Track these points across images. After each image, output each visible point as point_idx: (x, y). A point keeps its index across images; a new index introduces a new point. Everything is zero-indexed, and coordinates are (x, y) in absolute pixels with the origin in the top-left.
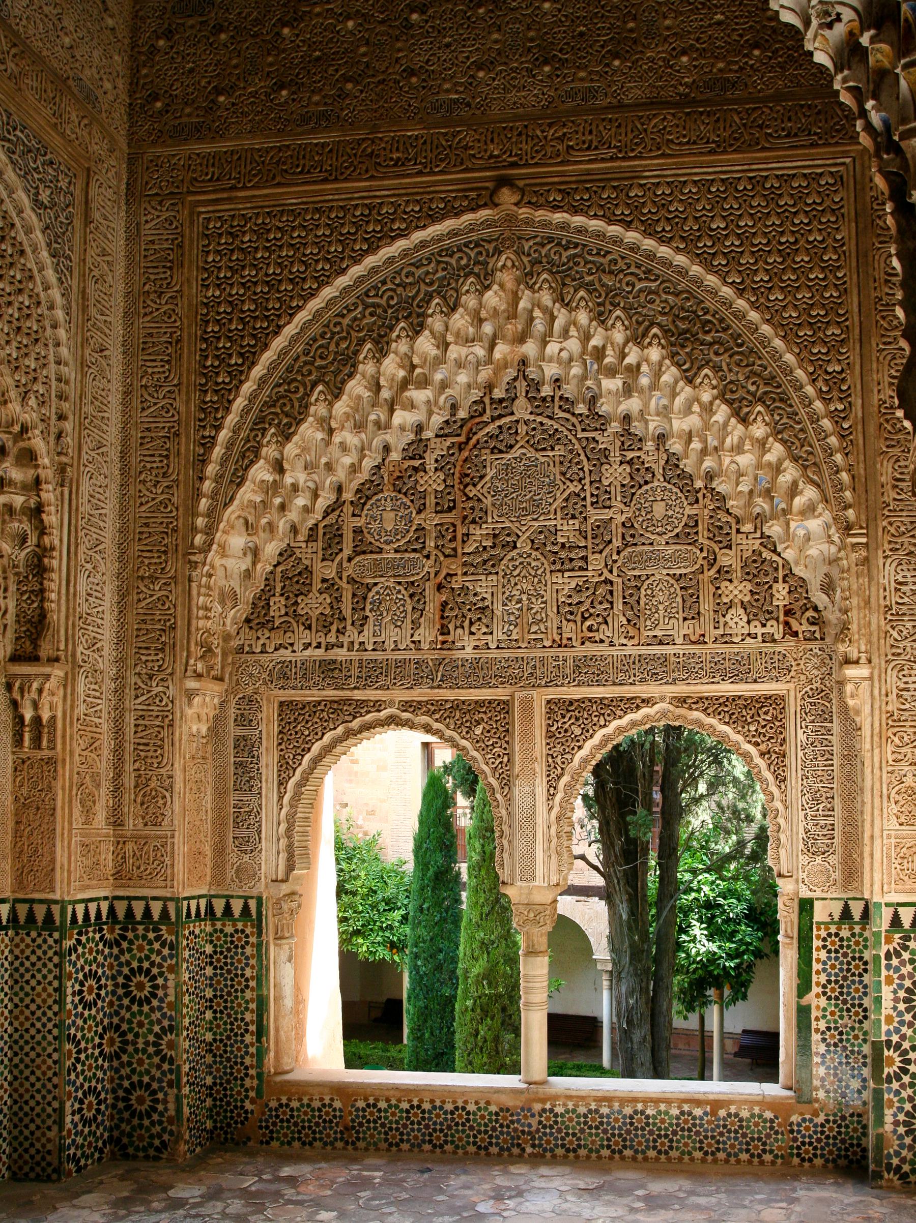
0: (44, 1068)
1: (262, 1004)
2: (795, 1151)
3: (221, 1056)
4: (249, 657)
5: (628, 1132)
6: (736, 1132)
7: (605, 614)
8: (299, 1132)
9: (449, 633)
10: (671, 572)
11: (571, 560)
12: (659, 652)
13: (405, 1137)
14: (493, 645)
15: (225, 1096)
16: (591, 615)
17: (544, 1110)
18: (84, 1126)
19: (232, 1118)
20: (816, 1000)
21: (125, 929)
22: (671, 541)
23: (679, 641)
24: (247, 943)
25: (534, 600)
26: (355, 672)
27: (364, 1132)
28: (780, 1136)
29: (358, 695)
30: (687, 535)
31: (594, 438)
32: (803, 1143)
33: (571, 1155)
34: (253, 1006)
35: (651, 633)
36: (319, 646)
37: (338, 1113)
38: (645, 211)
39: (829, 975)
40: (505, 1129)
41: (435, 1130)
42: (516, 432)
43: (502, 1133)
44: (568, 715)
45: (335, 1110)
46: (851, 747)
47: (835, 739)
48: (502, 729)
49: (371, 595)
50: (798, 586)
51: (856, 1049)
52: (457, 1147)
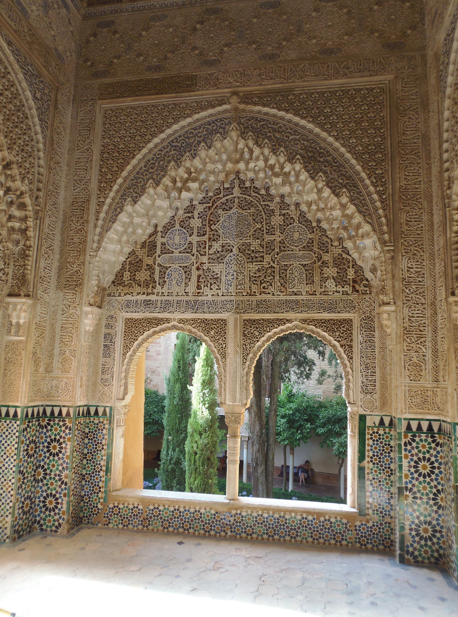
0: (7, 486)
2: (358, 540)
3: (89, 482)
5: (277, 526)
6: (329, 529)
7: (271, 281)
10: (301, 263)
11: (256, 257)
14: (220, 294)
15: (89, 501)
17: (237, 514)
18: (23, 515)
19: (92, 512)
21: (50, 420)
25: (239, 275)
26: (159, 305)
28: (350, 532)
29: (160, 316)
30: (308, 247)
32: (362, 536)
33: (249, 537)
34: (105, 458)
35: (291, 290)
37: (140, 511)
38: (295, 105)
39: (374, 452)
40: (218, 523)
41: (185, 522)
42: (234, 202)
43: (217, 524)
45: (139, 510)
46: (384, 344)
47: (376, 340)
48: (223, 332)
49: (167, 272)
50: (359, 270)
52: (195, 530)
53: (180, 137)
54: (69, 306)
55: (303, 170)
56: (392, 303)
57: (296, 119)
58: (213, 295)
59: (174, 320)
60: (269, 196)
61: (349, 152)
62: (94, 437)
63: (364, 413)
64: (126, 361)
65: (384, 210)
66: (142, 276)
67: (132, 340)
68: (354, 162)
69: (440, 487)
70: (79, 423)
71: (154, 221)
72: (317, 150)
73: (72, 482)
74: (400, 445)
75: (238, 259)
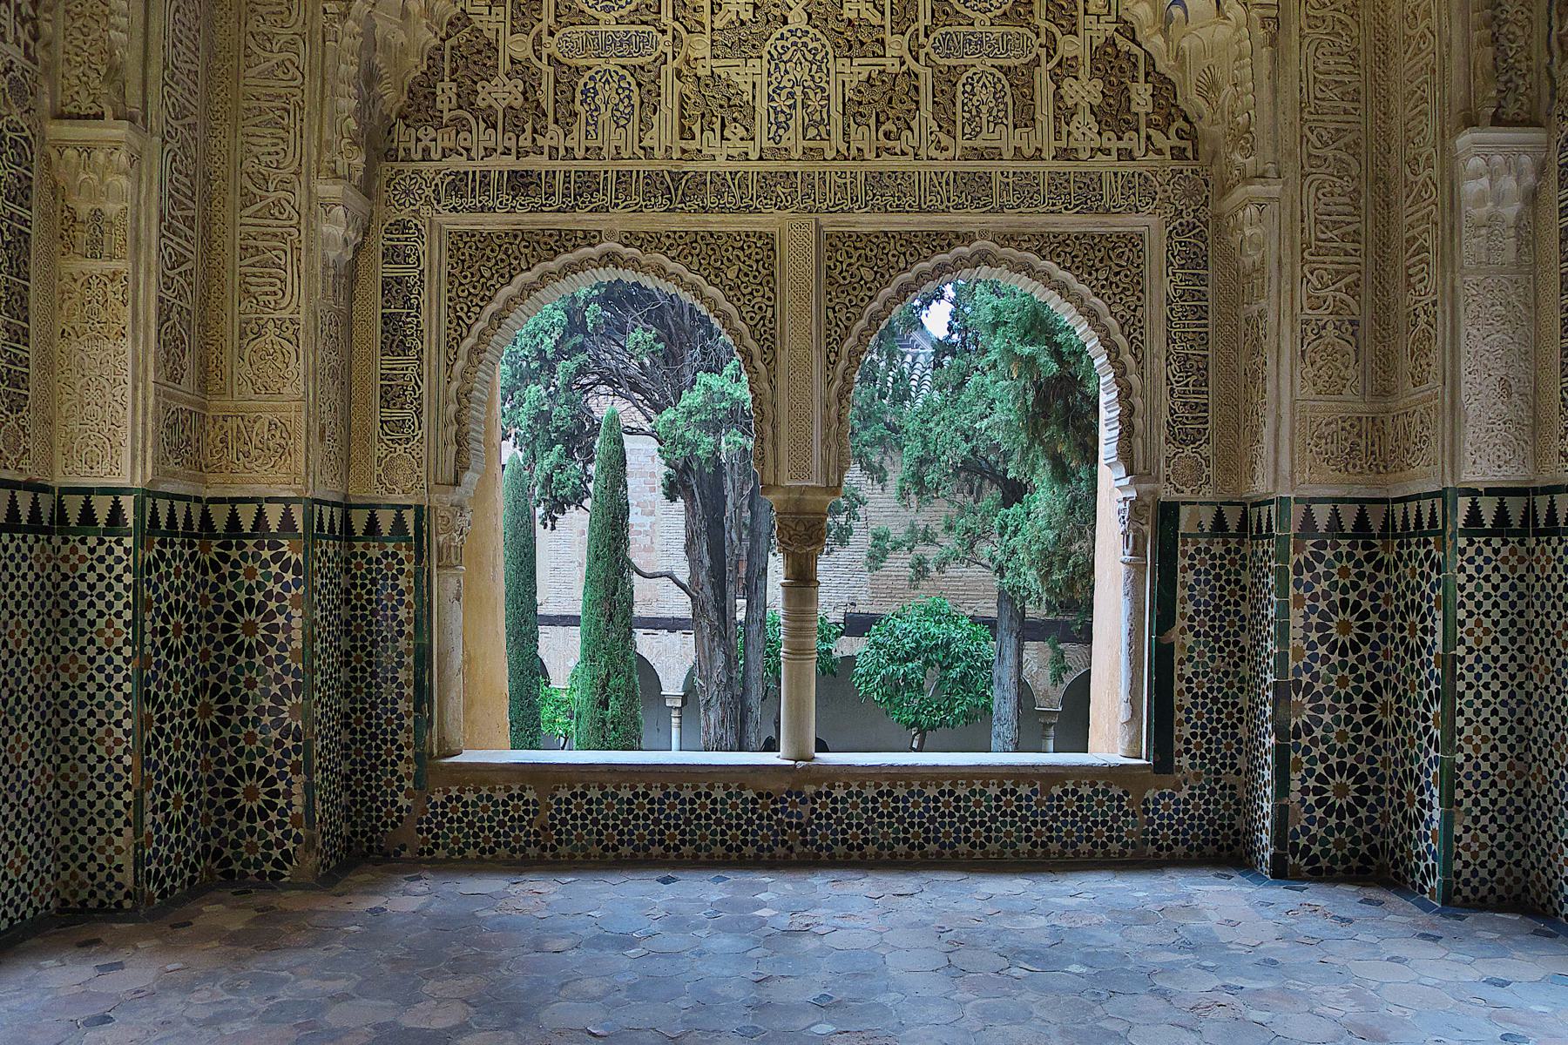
1: (423, 657)
2: (1150, 837)
4: (409, 168)
6: (1074, 814)
8: (476, 835)
9: (693, 138)
10: (997, 62)
11: (862, 44)
15: (369, 787)
16: (888, 119)
17: (819, 794)
19: (379, 818)
20: (1181, 638)
22: (996, 21)
24: (401, 571)
25: (812, 95)
27: (569, 833)
28: (1130, 818)
29: (564, 221)
32: (1161, 826)
34: (409, 660)
35: (968, 144)
36: (506, 152)
37: (531, 808)
40: (765, 822)
41: (668, 826)
43: (761, 827)
45: (526, 803)
48: (764, 272)
50: (1164, 88)
51: (1230, 700)
52: (699, 848)
56: (1272, 174)
58: (730, 158)
62: (369, 601)
63: (1175, 496)
64: (460, 364)
66: (501, 93)
69: (1380, 678)
73: (317, 728)
74: (1282, 574)
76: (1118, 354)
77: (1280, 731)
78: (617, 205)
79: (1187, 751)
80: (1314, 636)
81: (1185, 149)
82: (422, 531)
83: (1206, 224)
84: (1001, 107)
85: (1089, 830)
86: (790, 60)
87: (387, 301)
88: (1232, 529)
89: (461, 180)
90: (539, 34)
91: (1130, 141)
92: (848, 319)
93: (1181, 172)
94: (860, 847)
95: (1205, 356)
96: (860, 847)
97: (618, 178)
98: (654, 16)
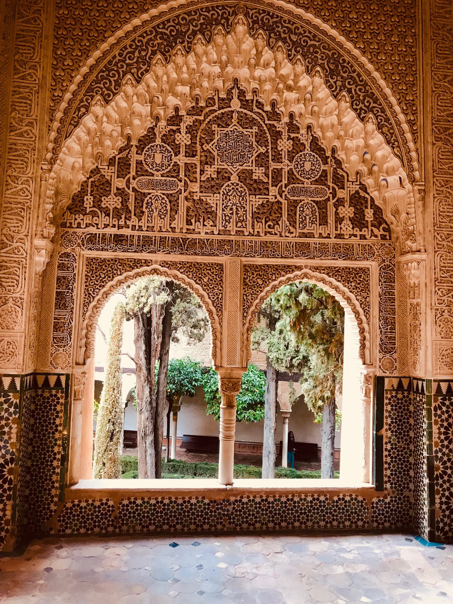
4: (71, 231)
5: (284, 512)
6: (343, 509)
9: (192, 224)
10: (313, 199)
11: (260, 189)
12: (306, 242)
13: (152, 522)
14: (216, 232)
16: (270, 220)
17: (236, 501)
20: (386, 433)
22: (313, 183)
23: (317, 236)
24: (58, 403)
28: (366, 511)
29: (137, 256)
30: (322, 180)
31: (274, 125)
32: (379, 514)
35: (301, 231)
36: (114, 226)
40: (213, 514)
41: (171, 516)
42: (232, 117)
43: (211, 516)
44: (255, 274)
45: (109, 507)
48: (219, 279)
49: (146, 199)
50: (378, 211)
51: (406, 459)
52: (184, 526)
53: (168, 21)
54: (12, 238)
55: (324, 86)
56: (423, 250)
57: (318, 21)
58: (207, 233)
59: (156, 262)
60: (275, 115)
61: (377, 70)
63: (383, 375)
65: (415, 143)
67: (97, 287)
68: (382, 83)
70: (27, 397)
71: (128, 131)
72: (340, 64)
75: (237, 189)
76: (359, 316)
77: (430, 475)
78: (160, 251)
79: (389, 481)
80: (443, 437)
81: (386, 236)
82: (69, 385)
83: (394, 265)
84: (314, 217)
85: (349, 516)
86: (231, 195)
87: (59, 286)
88: (406, 387)
89: (93, 237)
90: (129, 178)
91: (365, 232)
92: (252, 299)
93: (385, 244)
94: (253, 524)
95: (394, 318)
96: (253, 524)
97: (160, 239)
98: (177, 174)
